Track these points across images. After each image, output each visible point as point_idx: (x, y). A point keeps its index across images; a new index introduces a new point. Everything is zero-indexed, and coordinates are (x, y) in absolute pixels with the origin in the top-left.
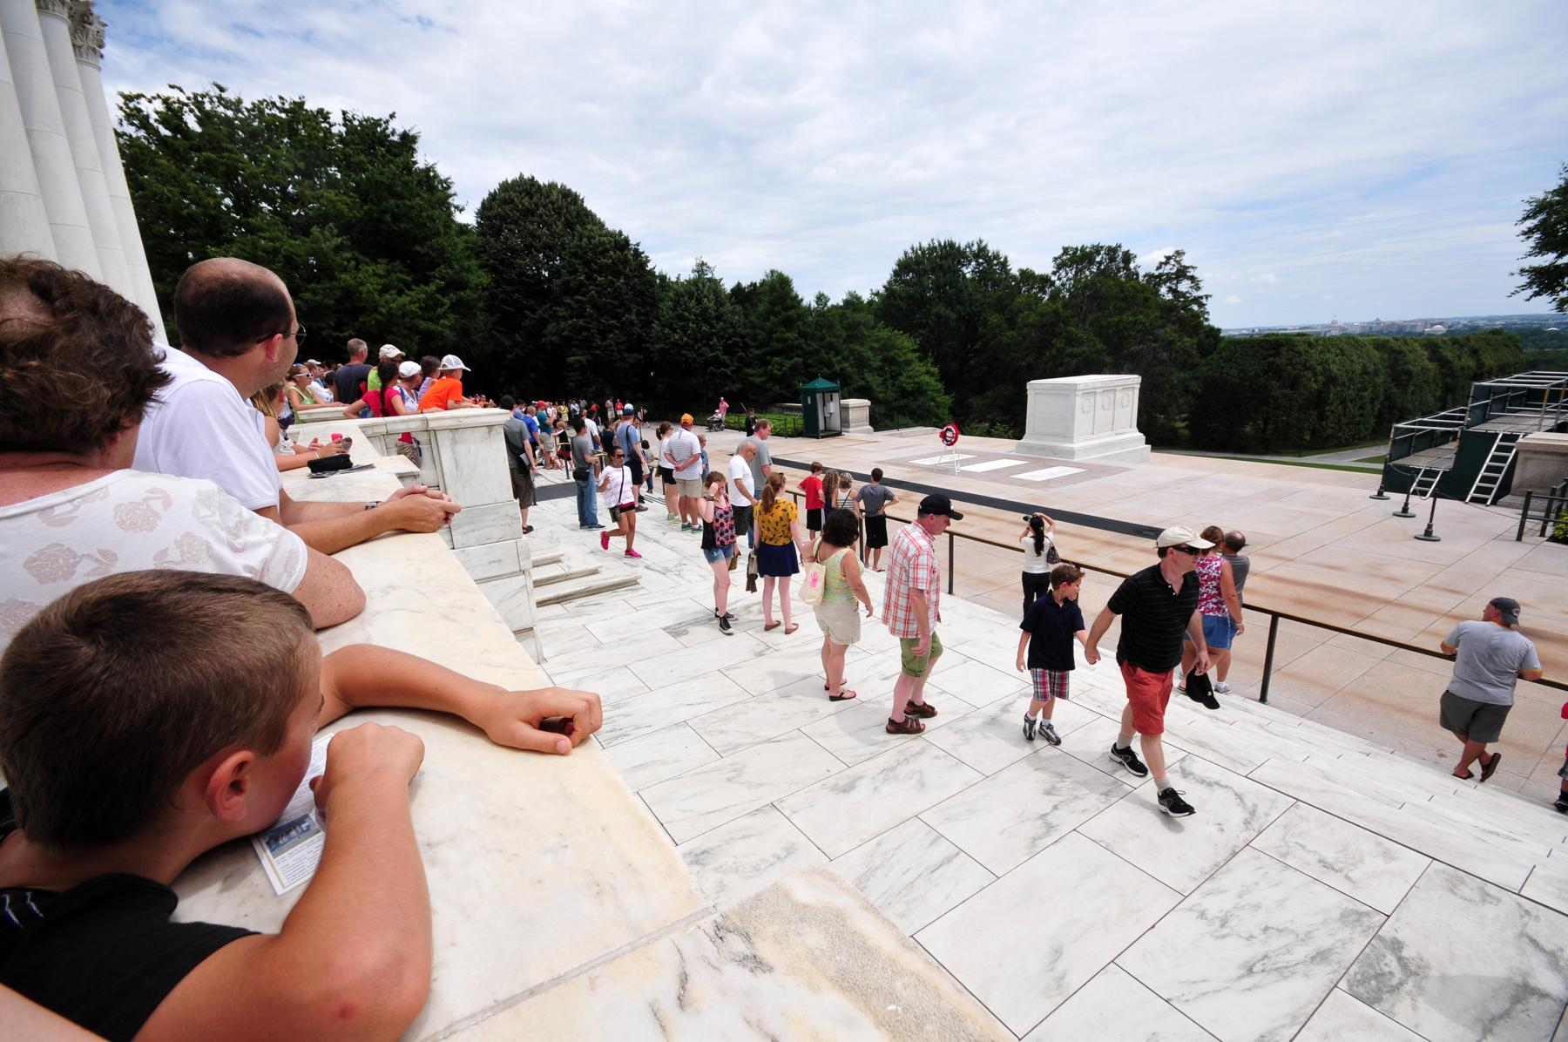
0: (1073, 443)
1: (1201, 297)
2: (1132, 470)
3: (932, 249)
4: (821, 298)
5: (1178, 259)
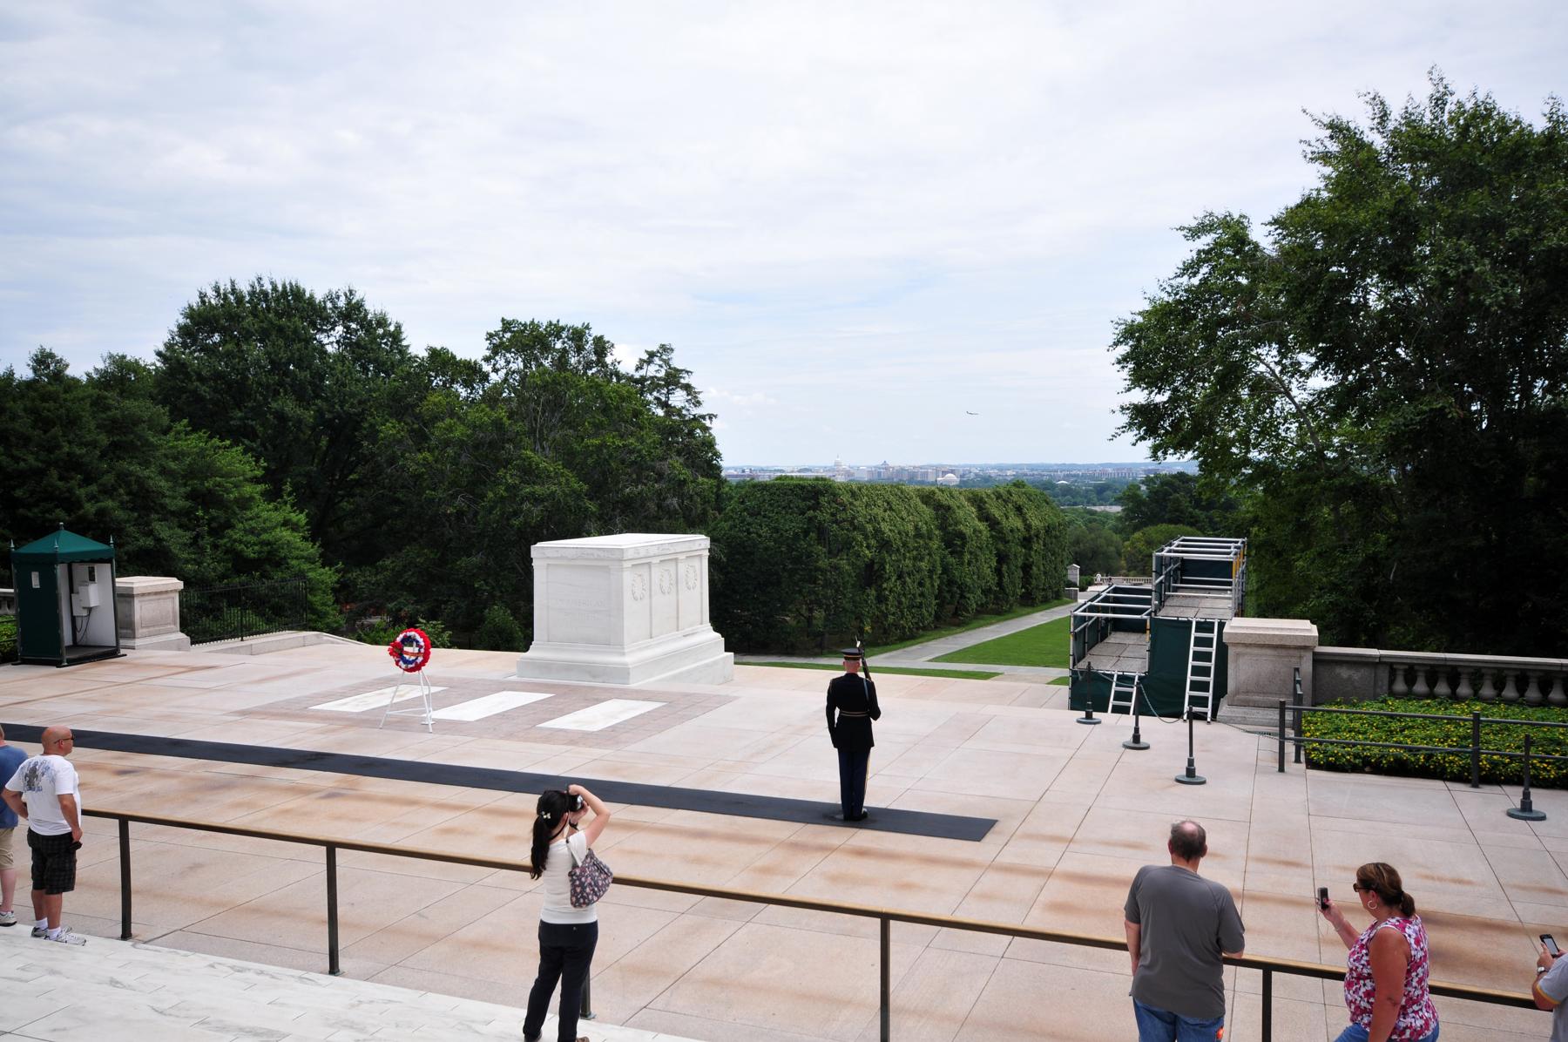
0: (623, 654)
1: (703, 417)
2: (736, 698)
3: (258, 295)
4: (408, 347)
5: (664, 357)
